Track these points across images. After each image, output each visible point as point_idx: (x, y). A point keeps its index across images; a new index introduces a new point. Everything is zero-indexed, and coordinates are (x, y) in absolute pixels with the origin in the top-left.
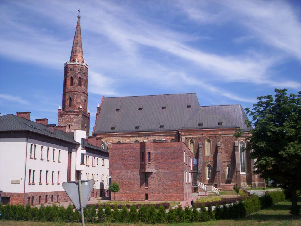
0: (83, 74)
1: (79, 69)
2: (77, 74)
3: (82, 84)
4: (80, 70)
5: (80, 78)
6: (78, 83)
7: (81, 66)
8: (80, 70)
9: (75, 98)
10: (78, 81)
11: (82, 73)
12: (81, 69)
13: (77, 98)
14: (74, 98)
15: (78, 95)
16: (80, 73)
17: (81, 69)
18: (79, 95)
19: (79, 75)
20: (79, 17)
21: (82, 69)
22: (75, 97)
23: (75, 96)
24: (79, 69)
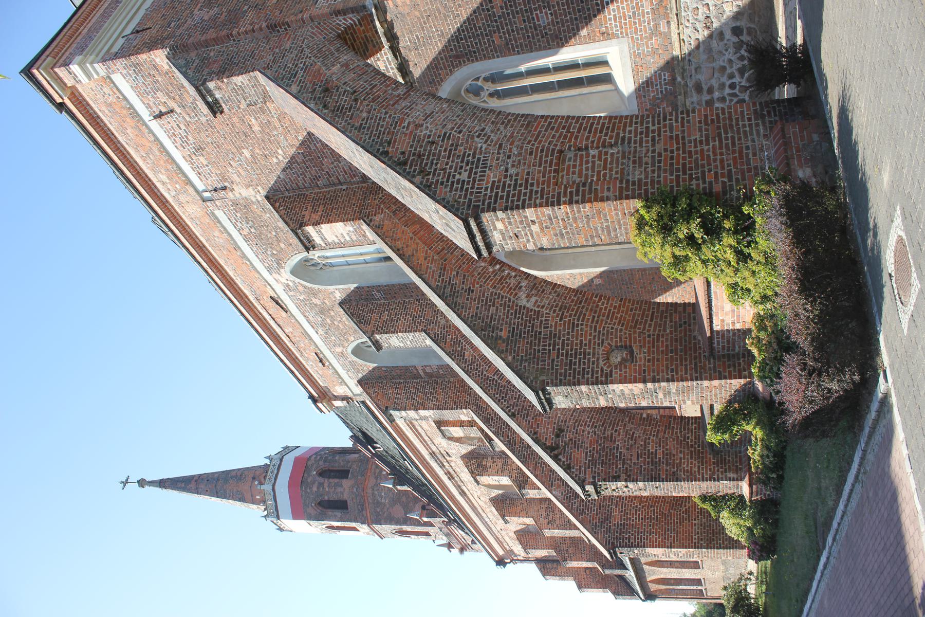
3: (334, 497)
20: (142, 483)
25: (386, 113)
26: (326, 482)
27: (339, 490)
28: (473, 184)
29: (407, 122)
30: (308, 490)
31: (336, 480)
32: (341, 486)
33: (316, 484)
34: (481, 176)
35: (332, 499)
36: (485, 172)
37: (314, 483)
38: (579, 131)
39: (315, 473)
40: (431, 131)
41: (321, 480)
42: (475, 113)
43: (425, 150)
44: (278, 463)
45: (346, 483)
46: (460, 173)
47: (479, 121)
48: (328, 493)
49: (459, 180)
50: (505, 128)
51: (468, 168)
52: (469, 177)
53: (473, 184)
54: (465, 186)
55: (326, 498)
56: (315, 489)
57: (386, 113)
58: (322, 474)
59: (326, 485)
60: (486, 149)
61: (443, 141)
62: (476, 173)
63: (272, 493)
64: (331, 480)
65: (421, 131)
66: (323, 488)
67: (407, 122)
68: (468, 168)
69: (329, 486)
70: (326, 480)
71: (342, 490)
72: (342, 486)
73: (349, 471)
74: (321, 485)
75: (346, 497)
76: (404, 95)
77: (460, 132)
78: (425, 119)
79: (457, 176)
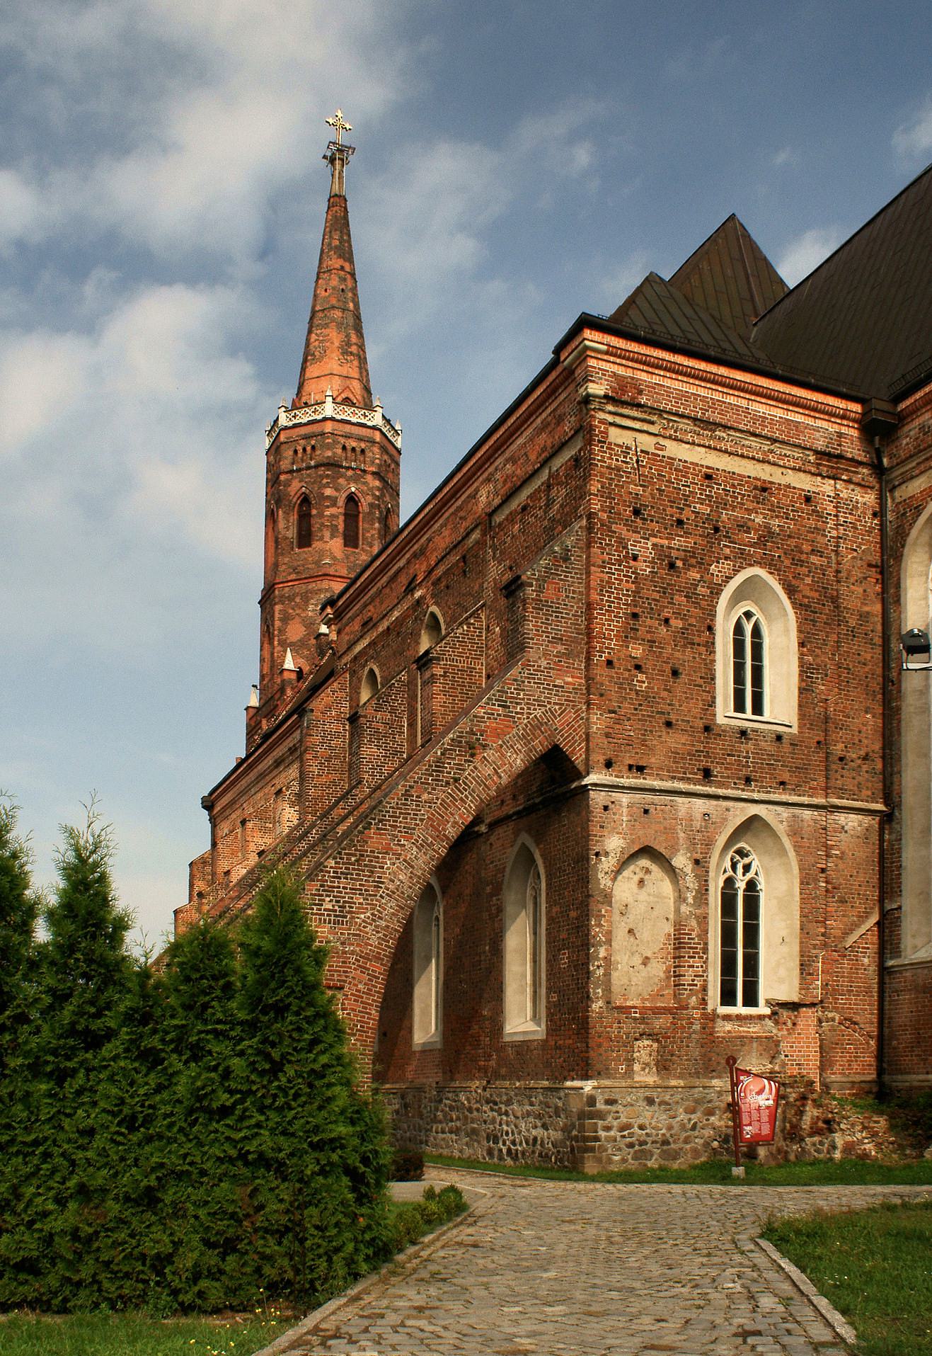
0: (321, 471)
1: (296, 452)
2: (288, 483)
3: (315, 527)
4: (304, 450)
5: (305, 500)
6: (292, 533)
7: (303, 431)
8: (304, 450)
9: (277, 624)
10: (294, 517)
11: (316, 467)
12: (309, 448)
13: (286, 619)
14: (273, 626)
15: (291, 599)
16: (299, 470)
17: (309, 448)
18: (298, 600)
19: (295, 487)
21: (313, 442)
22: (277, 615)
23: (278, 608)
24: (296, 452)
25: (422, 820)
26: (338, 510)
27: (327, 534)
28: (316, 914)
29: (406, 843)
30: (325, 481)
31: (341, 528)
32: (332, 537)
33: (335, 494)
34: (325, 920)
35: (313, 521)
36: (330, 923)
37: (337, 490)
38: (362, 1002)
39: (353, 489)
40: (388, 868)
41: (341, 502)
42: (403, 908)
43: (366, 866)
44: (369, 424)
45: (335, 545)
46: (331, 901)
47: (393, 914)
48: (321, 515)
49: (324, 900)
50: (379, 938)
51: (336, 908)
52: (325, 910)
53: (316, 914)
54: (315, 907)
55: (314, 512)
56: (328, 492)
57: (422, 820)
58: (351, 499)
59: (333, 510)
60: (356, 923)
61: (374, 881)
62: (328, 915)
63: (320, 417)
64: (341, 518)
65: (390, 859)
66: (328, 507)
67: (406, 843)
68: (336, 908)
69: (332, 516)
70: (342, 510)
71: (327, 538)
72: (331, 539)
73: (356, 546)
74: (334, 502)
75: (317, 545)
76: (444, 835)
77: (381, 896)
78: (405, 860)
79: (328, 899)
